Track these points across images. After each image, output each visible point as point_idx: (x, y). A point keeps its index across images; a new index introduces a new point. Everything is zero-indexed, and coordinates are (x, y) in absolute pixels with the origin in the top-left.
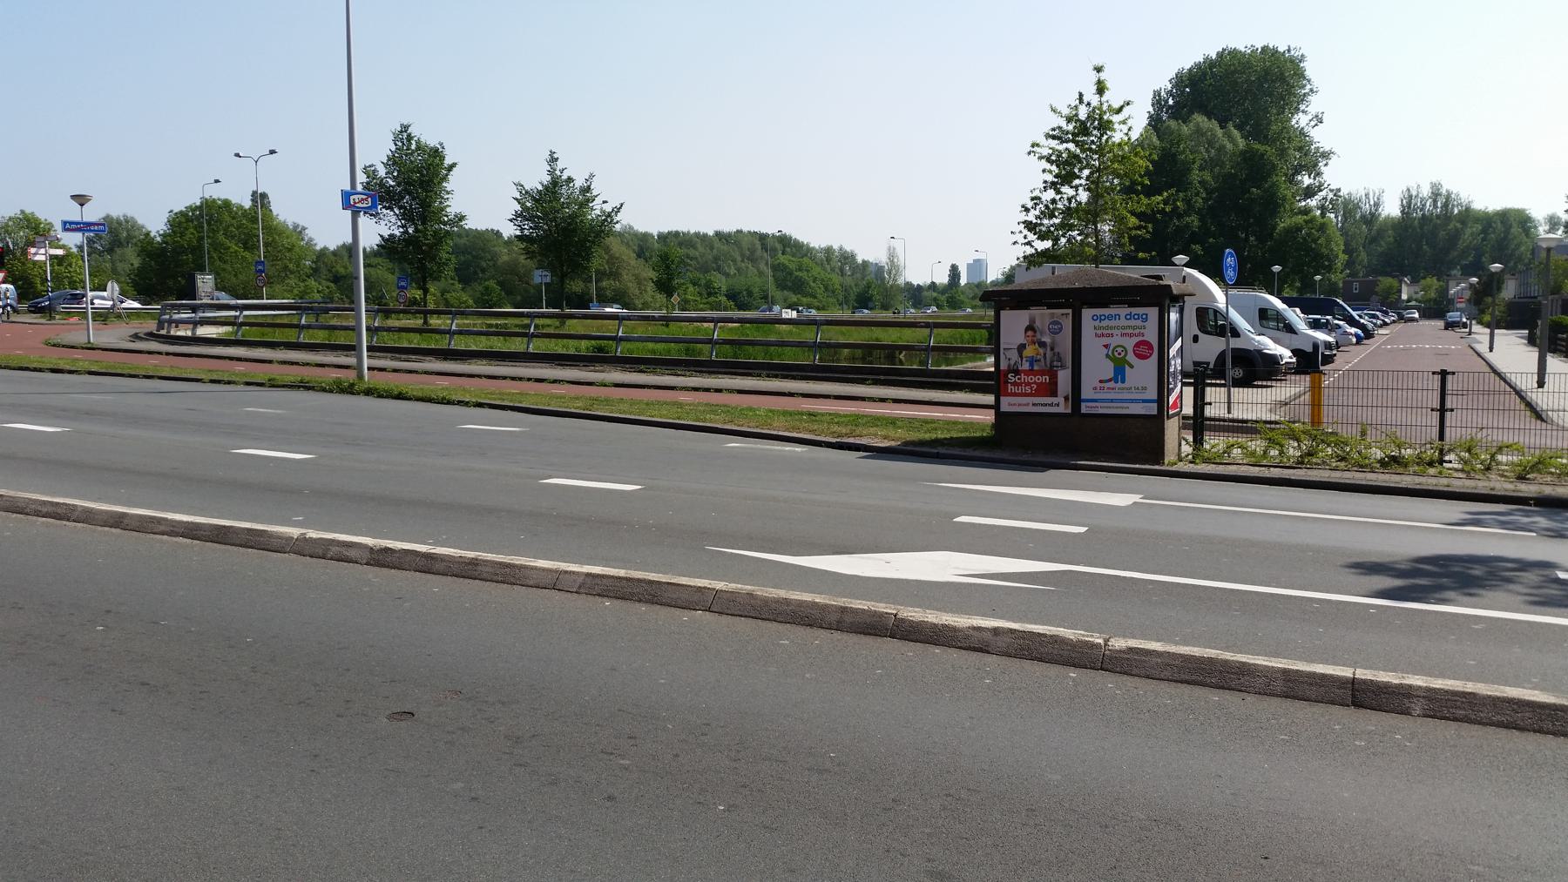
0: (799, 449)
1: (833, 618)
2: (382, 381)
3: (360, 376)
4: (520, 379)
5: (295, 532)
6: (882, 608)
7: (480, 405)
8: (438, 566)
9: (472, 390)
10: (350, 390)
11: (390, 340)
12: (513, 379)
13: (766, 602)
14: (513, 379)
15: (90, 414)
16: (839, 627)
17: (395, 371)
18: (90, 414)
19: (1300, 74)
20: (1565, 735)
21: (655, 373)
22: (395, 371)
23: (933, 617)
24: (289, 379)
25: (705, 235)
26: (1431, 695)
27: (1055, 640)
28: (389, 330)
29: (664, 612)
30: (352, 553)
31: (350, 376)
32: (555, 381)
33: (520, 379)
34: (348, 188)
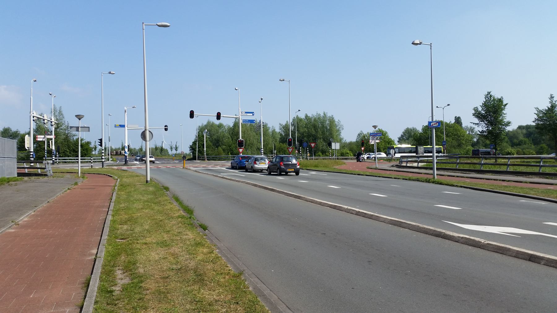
0: (544, 203)
1: (431, 232)
2: (442, 179)
3: (434, 178)
4: (497, 180)
5: (346, 207)
6: (477, 239)
7: (461, 187)
8: (366, 216)
9: (461, 182)
10: (428, 181)
11: (443, 166)
12: (495, 180)
13: (421, 228)
14: (495, 180)
15: (349, 185)
16: (432, 235)
17: (457, 177)
18: (349, 185)
19: (332, 121)
20: (556, 268)
21: (552, 179)
22: (457, 177)
23: (451, 234)
24: (414, 178)
25: (528, 127)
26: (548, 260)
27: (474, 240)
28: (462, 163)
29: (402, 229)
30: (353, 212)
31: (431, 177)
32: (509, 181)
33: (497, 180)
34: (431, 120)
